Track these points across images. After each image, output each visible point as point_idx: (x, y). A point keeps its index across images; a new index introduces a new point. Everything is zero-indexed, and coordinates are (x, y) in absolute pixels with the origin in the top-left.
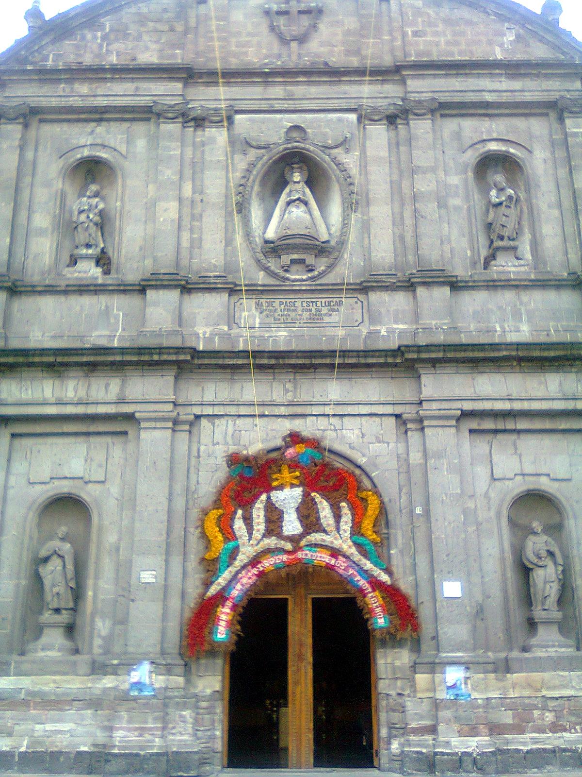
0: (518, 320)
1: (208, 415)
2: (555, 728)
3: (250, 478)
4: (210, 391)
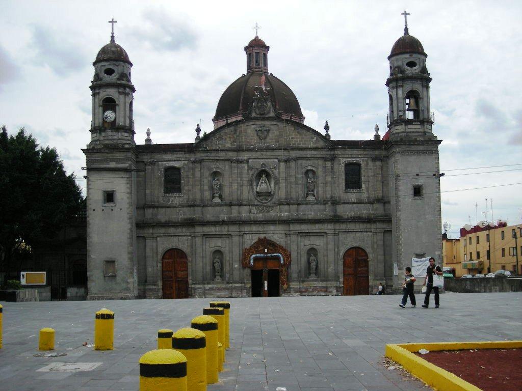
0: (310, 212)
2: (312, 292)
3: (256, 247)
4: (246, 229)
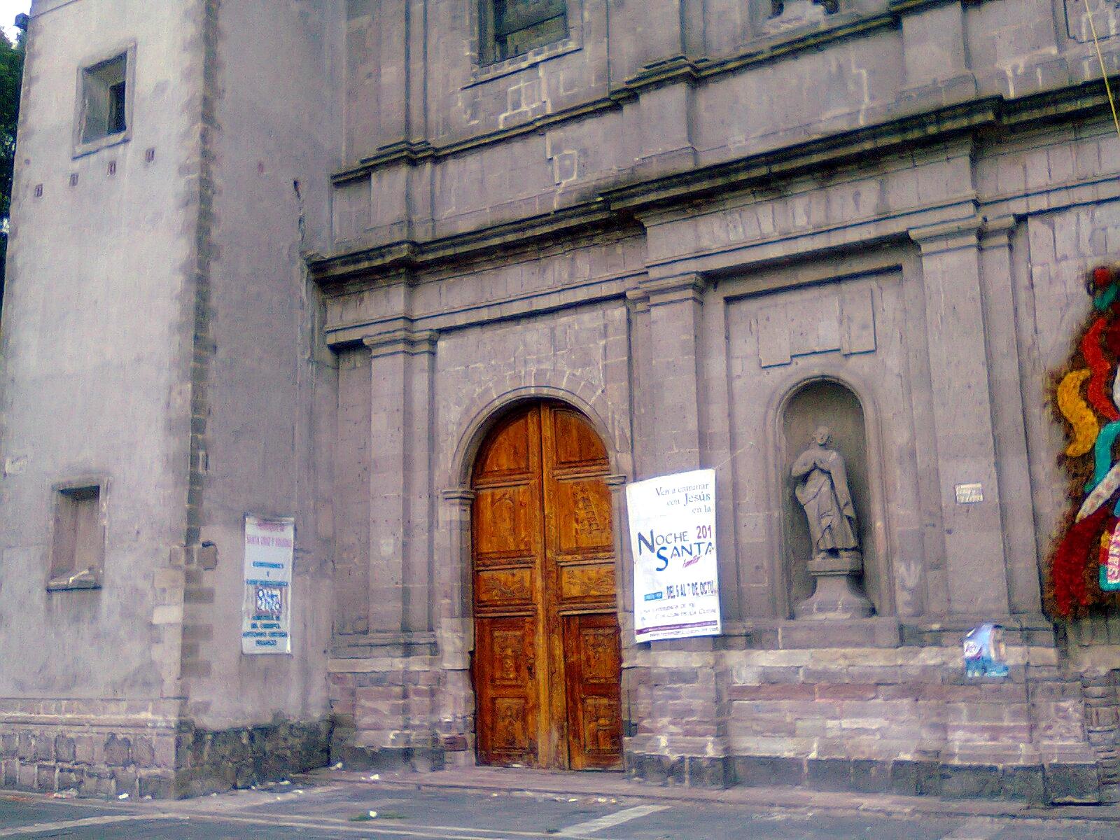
1: (1041, 212)
4: (1037, 169)
